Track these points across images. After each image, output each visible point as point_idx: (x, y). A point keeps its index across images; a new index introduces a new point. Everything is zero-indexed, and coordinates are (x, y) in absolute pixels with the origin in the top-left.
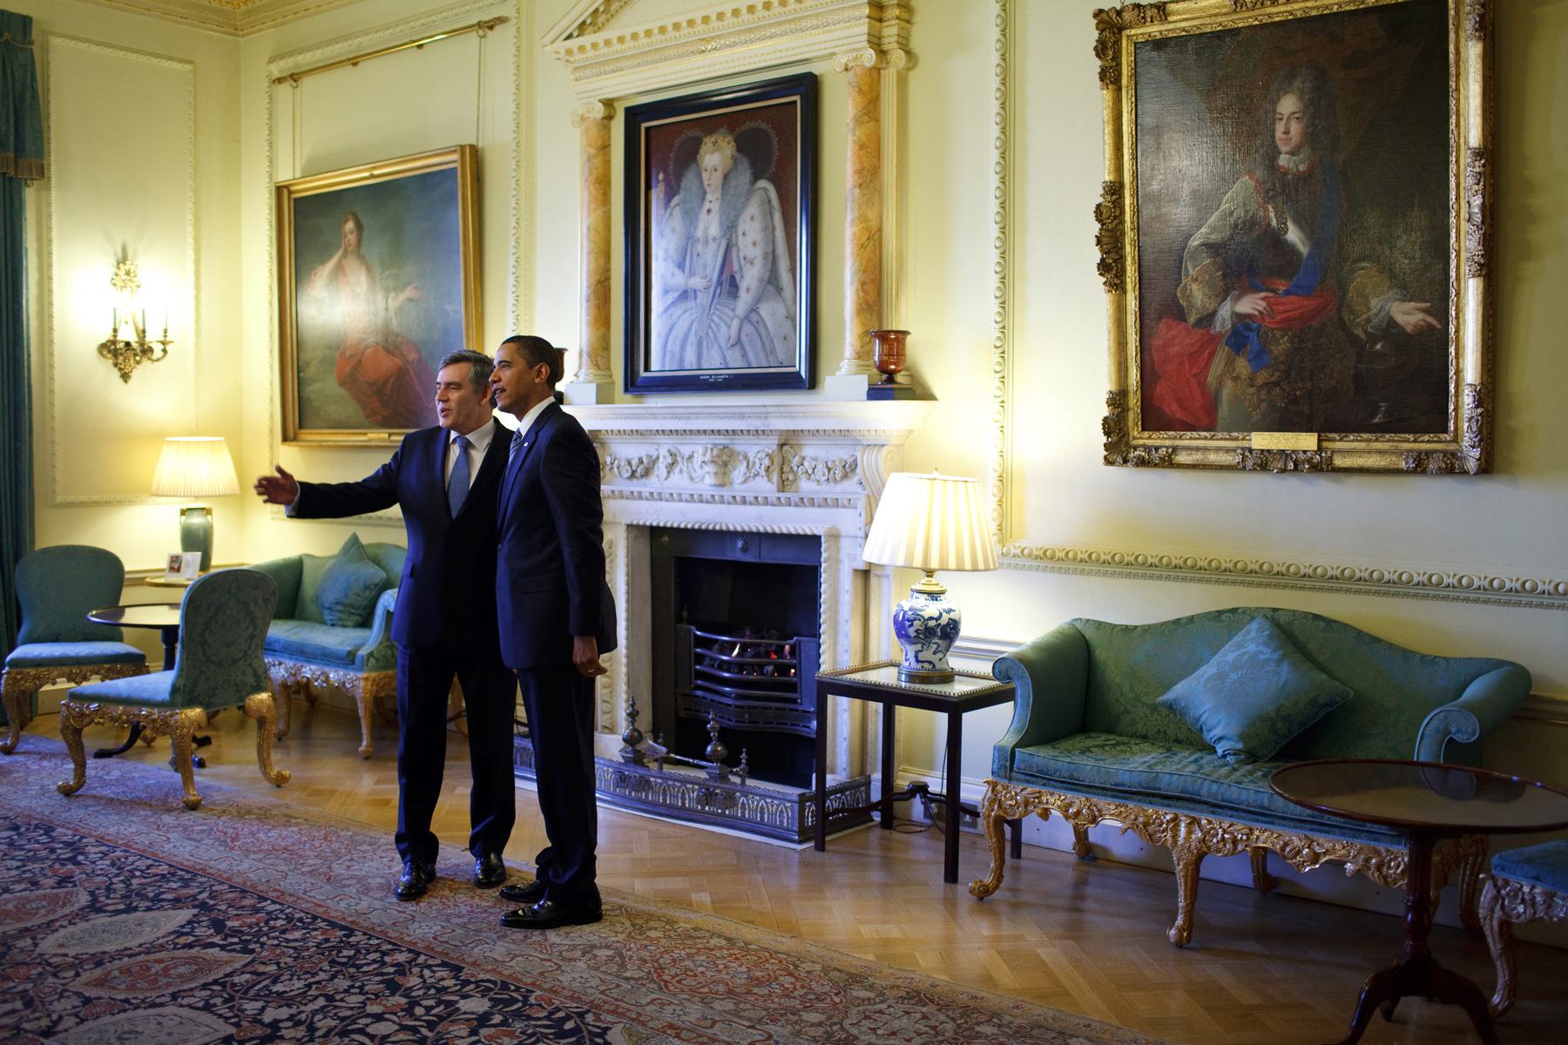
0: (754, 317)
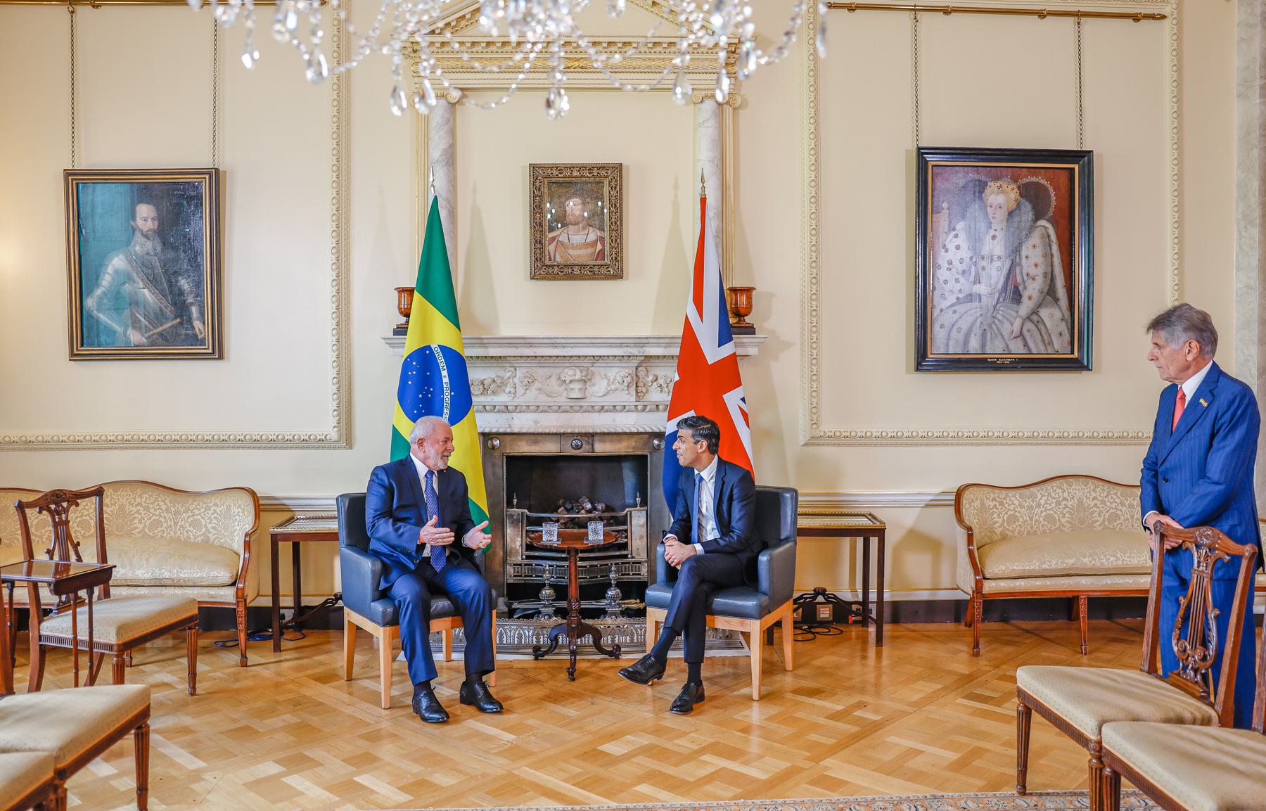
0: (1035, 318)
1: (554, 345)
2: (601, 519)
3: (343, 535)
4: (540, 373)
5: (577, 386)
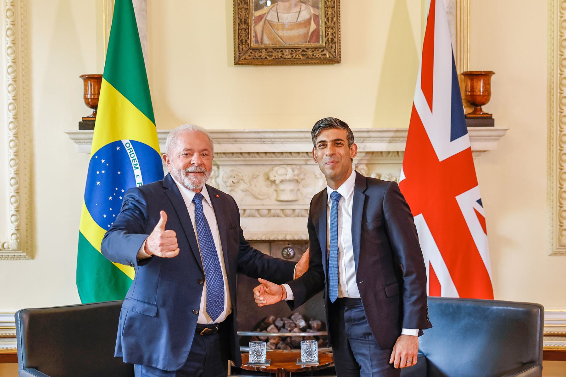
1: (262, 140)
2: (316, 338)
3: (22, 357)
4: (246, 172)
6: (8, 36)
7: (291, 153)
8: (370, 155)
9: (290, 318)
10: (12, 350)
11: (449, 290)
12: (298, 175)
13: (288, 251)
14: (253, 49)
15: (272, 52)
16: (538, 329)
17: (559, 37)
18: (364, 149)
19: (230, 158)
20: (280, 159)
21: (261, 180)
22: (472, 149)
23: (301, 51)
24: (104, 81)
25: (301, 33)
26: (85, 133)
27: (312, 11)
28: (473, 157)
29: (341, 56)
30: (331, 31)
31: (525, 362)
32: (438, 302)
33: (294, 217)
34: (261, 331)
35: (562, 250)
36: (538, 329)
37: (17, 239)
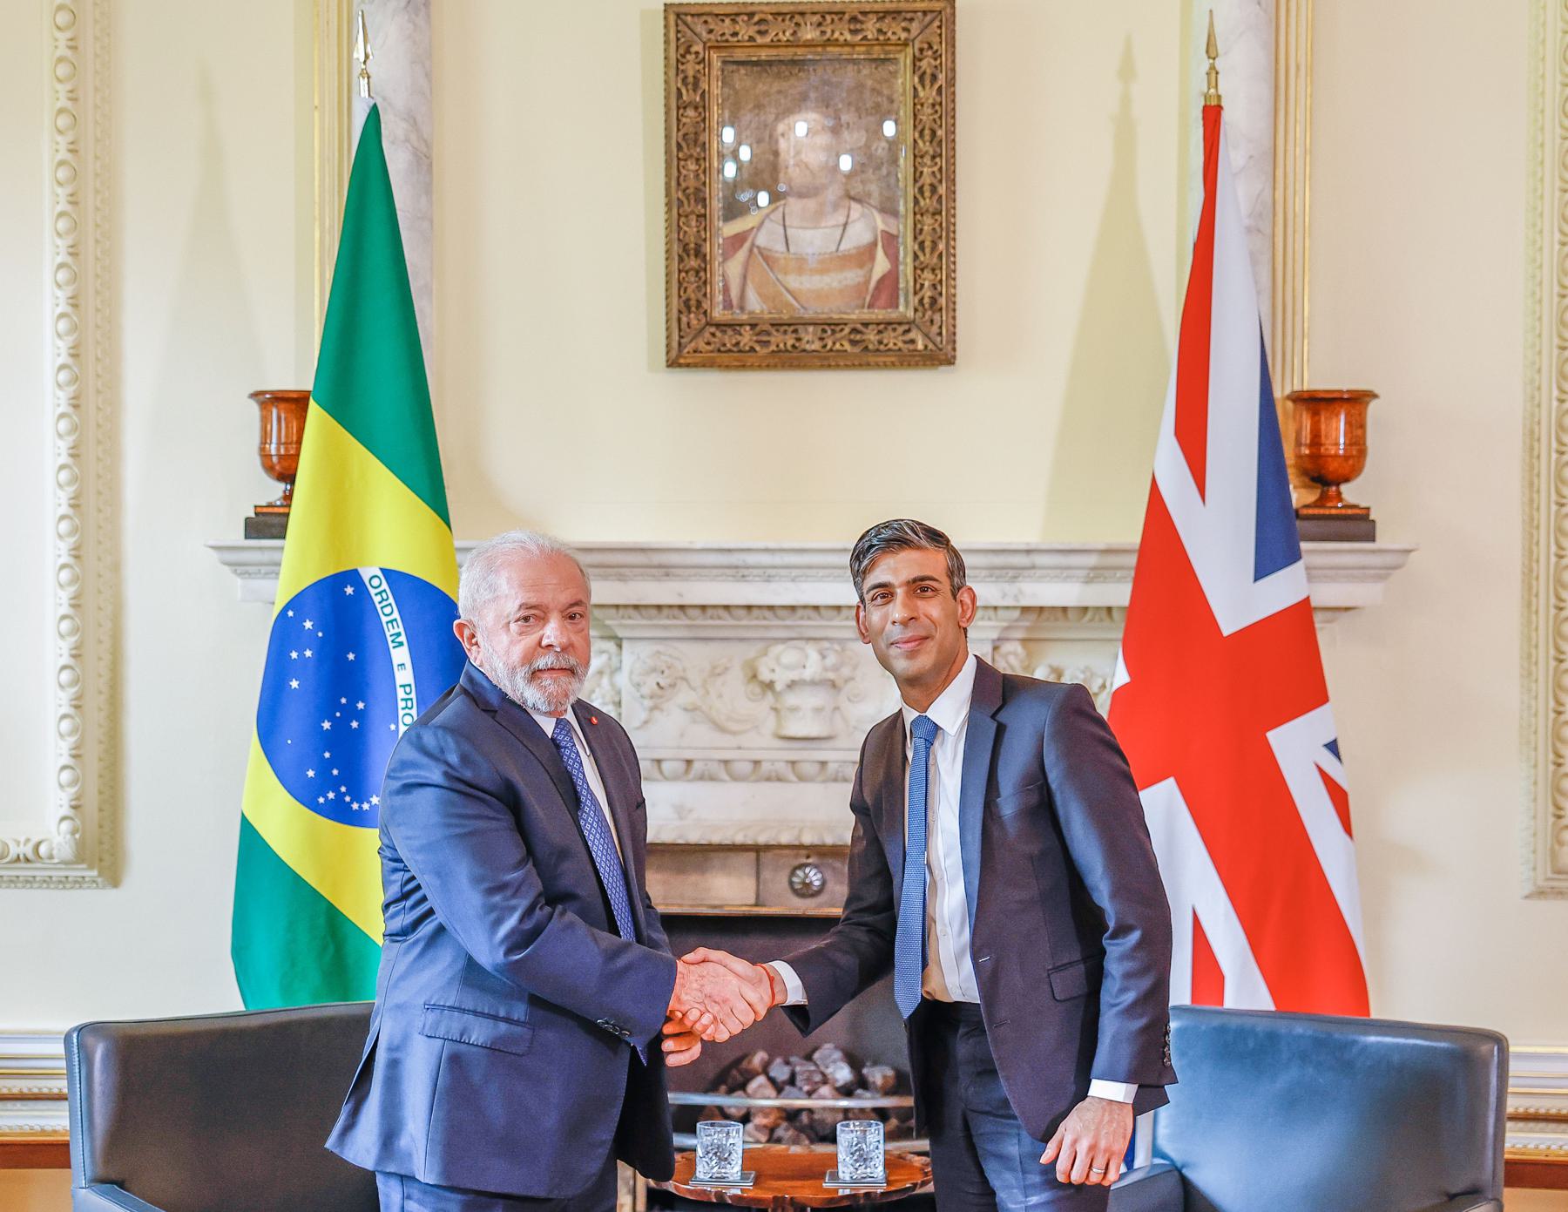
1: (739, 573)
2: (882, 1114)
4: (695, 657)
5: (808, 700)
6: (59, 286)
7: (816, 608)
8: (1033, 616)
9: (808, 1057)
10: (55, 1132)
11: (1246, 990)
12: (836, 669)
13: (807, 876)
14: (718, 326)
15: (769, 334)
16: (1493, 1099)
17: (1556, 299)
18: (1016, 598)
19: (650, 618)
20: (788, 623)
21: (735, 681)
22: (1314, 603)
23: (847, 330)
24: (312, 405)
25: (849, 282)
26: (260, 548)
27: (880, 222)
28: (1317, 626)
29: (958, 346)
30: (931, 276)
31: (1454, 1190)
32: (1216, 1022)
33: (824, 781)
34: (730, 1091)
35: (1562, 882)
36: (1493, 1099)
37: (73, 833)
